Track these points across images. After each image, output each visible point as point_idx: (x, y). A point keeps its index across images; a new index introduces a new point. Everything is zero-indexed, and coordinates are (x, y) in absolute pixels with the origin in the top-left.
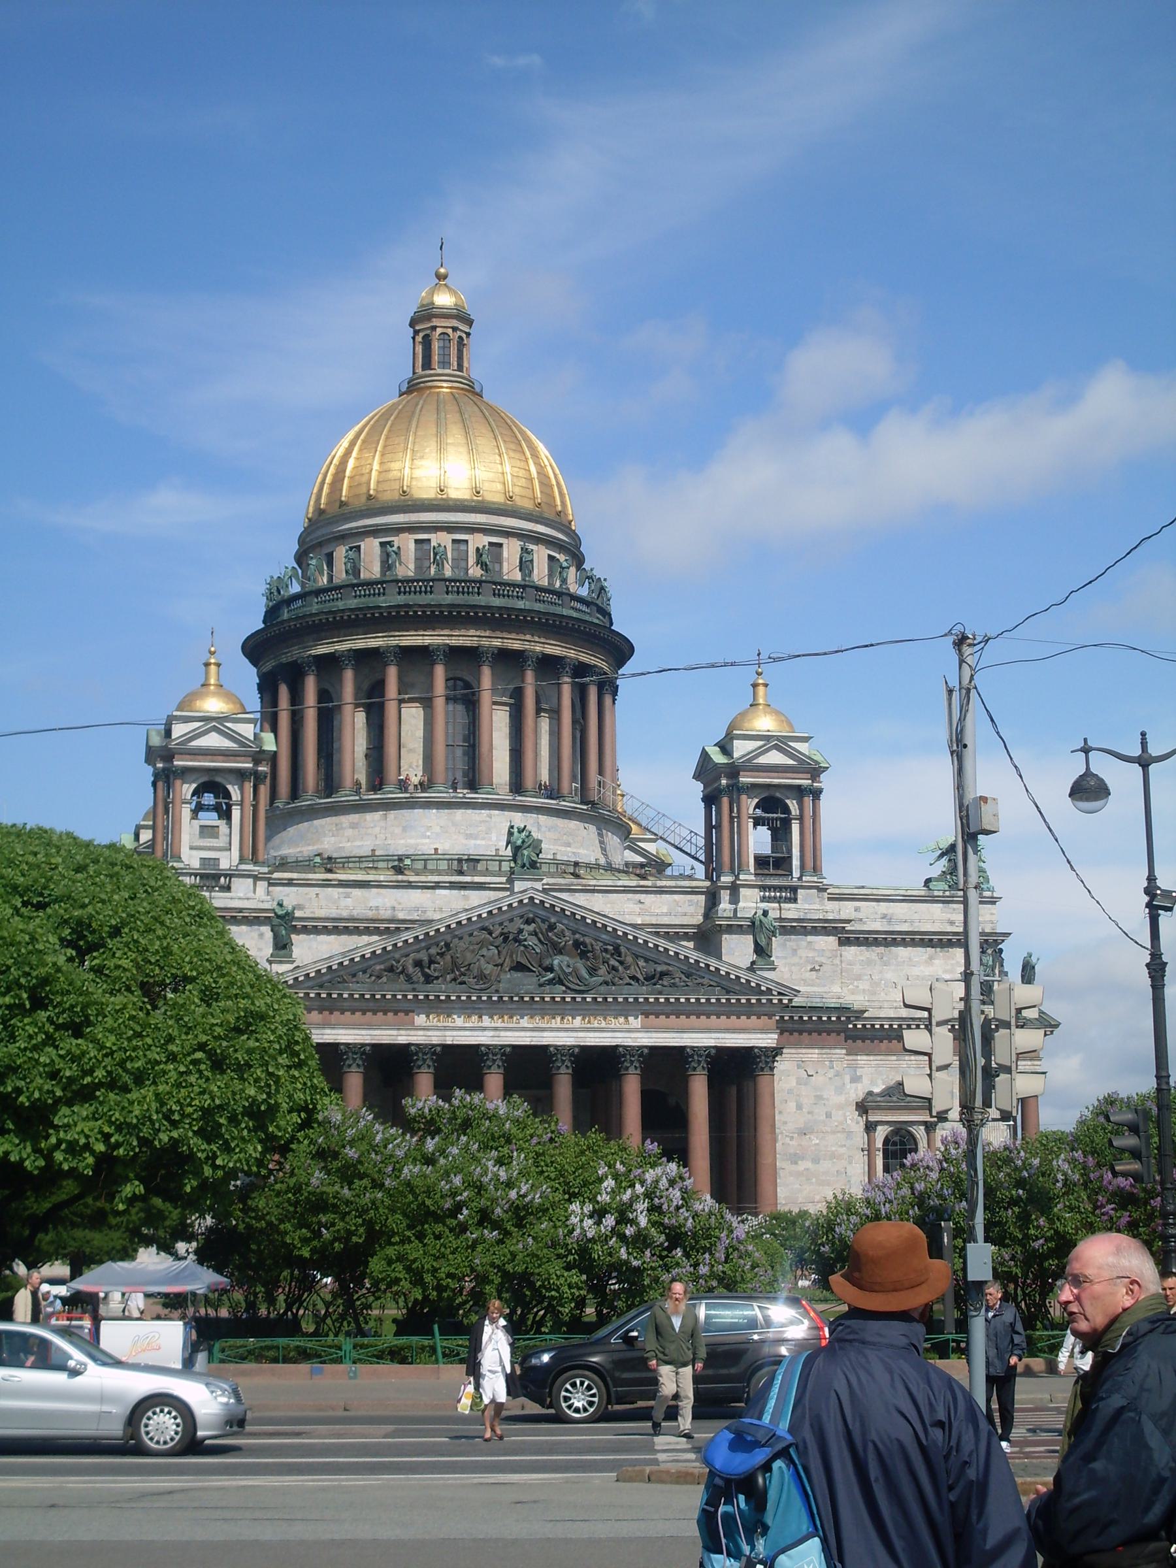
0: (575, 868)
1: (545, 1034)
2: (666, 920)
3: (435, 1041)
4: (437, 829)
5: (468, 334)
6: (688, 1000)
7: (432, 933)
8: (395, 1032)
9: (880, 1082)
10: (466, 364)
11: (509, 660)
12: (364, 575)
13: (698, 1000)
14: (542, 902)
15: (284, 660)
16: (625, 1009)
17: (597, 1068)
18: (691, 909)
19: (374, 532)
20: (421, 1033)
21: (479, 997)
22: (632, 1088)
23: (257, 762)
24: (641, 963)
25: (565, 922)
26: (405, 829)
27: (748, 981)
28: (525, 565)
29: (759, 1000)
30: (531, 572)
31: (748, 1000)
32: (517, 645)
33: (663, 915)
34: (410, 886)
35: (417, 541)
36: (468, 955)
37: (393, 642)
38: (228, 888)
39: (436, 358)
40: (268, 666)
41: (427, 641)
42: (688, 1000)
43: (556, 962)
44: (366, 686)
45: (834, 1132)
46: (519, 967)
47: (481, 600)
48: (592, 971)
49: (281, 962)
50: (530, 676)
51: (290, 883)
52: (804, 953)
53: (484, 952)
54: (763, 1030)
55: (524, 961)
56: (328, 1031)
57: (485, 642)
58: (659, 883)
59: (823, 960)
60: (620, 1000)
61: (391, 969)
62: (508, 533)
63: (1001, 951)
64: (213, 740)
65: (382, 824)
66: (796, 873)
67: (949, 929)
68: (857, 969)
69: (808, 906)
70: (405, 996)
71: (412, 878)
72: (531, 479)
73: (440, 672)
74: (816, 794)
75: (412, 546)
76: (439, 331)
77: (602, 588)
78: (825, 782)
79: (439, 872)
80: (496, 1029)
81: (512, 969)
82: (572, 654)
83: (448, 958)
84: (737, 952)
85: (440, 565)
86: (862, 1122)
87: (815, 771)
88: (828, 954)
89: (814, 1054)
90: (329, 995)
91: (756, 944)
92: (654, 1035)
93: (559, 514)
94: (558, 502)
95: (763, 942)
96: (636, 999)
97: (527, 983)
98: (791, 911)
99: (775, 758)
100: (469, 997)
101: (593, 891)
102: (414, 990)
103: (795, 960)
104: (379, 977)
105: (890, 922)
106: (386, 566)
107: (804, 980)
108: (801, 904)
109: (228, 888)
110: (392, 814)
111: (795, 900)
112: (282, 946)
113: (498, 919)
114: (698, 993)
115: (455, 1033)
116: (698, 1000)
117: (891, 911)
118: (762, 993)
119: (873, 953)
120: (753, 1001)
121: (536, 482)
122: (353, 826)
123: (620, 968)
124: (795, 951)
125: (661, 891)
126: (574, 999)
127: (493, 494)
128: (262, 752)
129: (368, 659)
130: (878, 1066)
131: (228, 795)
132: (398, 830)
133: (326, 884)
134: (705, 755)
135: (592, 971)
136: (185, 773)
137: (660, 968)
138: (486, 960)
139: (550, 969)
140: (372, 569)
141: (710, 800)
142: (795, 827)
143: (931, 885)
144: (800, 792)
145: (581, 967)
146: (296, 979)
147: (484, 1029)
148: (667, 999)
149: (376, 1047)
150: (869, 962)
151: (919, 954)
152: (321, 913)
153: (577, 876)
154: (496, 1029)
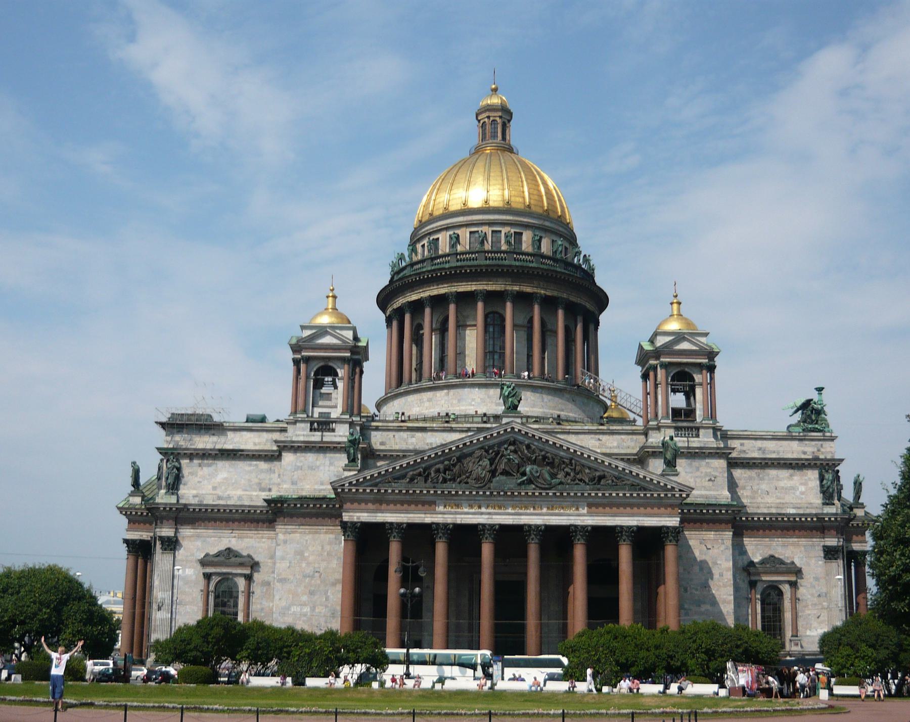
0: (559, 420)
1: (523, 517)
2: (616, 451)
3: (449, 521)
4: (479, 400)
5: (509, 121)
6: (618, 494)
7: (447, 451)
8: (423, 515)
9: (758, 555)
10: (508, 138)
11: (523, 300)
12: (440, 252)
13: (624, 494)
14: (520, 431)
15: (395, 306)
16: (576, 502)
17: (558, 540)
18: (632, 444)
19: (447, 228)
20: (440, 516)
21: (477, 493)
22: (579, 552)
23: (353, 353)
24: (587, 471)
25: (536, 443)
26: (459, 401)
27: (659, 483)
28: (538, 242)
29: (666, 495)
30: (539, 247)
31: (659, 495)
32: (528, 290)
33: (614, 447)
34: (451, 430)
35: (471, 233)
36: (471, 464)
37: (454, 289)
38: (333, 430)
39: (488, 135)
40: (388, 313)
41: (474, 288)
42: (618, 494)
43: (528, 469)
44: (440, 320)
45: (725, 586)
46: (505, 473)
47: (506, 262)
48: (553, 476)
49: (350, 470)
50: (536, 308)
51: (377, 429)
52: (702, 469)
53: (481, 463)
54: (670, 515)
55: (507, 469)
56: (380, 515)
57: (509, 288)
58: (611, 428)
59: (717, 474)
60: (572, 494)
61: (420, 474)
62: (527, 226)
63: (838, 471)
64: (327, 340)
65: (446, 398)
66: (698, 420)
67: (803, 456)
69: (706, 439)
70: (428, 492)
71: (454, 425)
72: (541, 196)
73: (480, 305)
74: (711, 369)
75: (468, 235)
76: (491, 119)
77: (586, 260)
78: (718, 360)
79: (472, 423)
80: (489, 514)
81: (502, 474)
82: (565, 296)
83: (457, 467)
84: (657, 466)
85: (482, 243)
86: (746, 582)
87: (711, 355)
88: (720, 470)
89: (711, 535)
90: (379, 491)
91: (665, 459)
92: (596, 518)
93: (560, 217)
94: (559, 210)
96: (582, 494)
97: (510, 483)
98: (695, 443)
99: (685, 346)
100: (471, 492)
101: (569, 433)
102: (434, 487)
103: (698, 474)
104: (412, 480)
105: (764, 453)
106: (453, 246)
107: (704, 487)
108: (701, 438)
109: (333, 430)
110: (452, 392)
111: (698, 436)
112: (352, 460)
113: (491, 442)
114: (624, 489)
115: (462, 516)
116: (624, 494)
117: (764, 446)
118: (669, 490)
119: (753, 473)
120: (662, 495)
121: (544, 198)
122: (430, 400)
123: (572, 474)
124: (698, 469)
125: (612, 433)
126: (540, 494)
127: (517, 203)
128: (356, 347)
129: (439, 302)
130: (757, 545)
131: (336, 374)
132: (455, 402)
133: (399, 429)
134: (641, 347)
135: (553, 476)
136: (307, 360)
137: (598, 474)
138: (480, 468)
139: (524, 474)
140: (444, 246)
141: (645, 377)
142: (699, 391)
143: (791, 429)
144: (700, 365)
145: (546, 471)
146: (357, 481)
147: (482, 514)
148: (603, 494)
149: (411, 526)
150: (751, 478)
151: (784, 473)
152: (397, 447)
153: (559, 424)
154: (489, 514)
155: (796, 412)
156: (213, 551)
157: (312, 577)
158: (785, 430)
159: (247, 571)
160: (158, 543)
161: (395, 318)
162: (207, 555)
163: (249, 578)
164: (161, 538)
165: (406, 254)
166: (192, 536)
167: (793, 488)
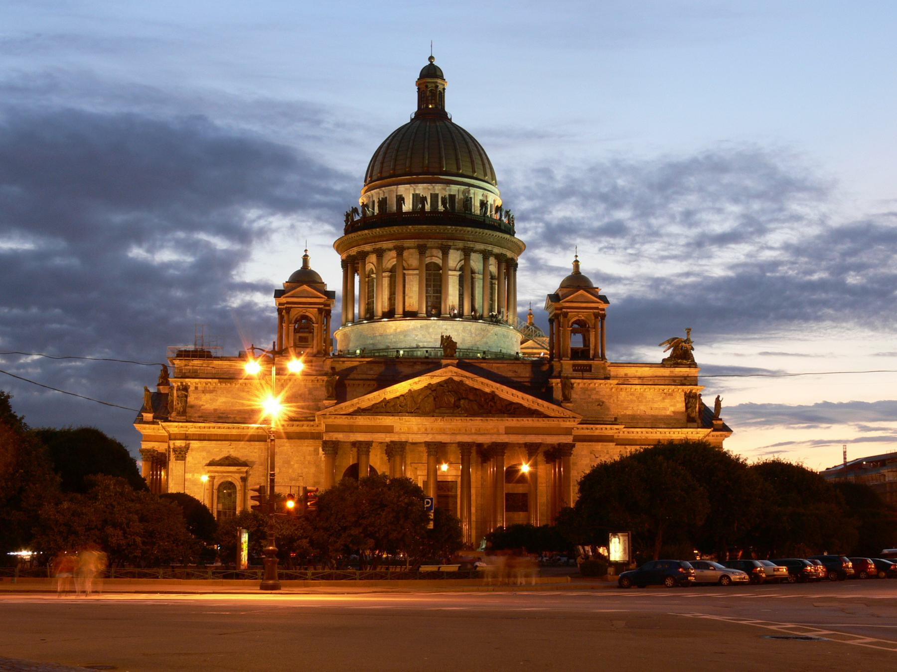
5: (444, 89)
68: (625, 404)
95: (567, 392)
115: (413, 436)
135: (481, 406)
155: (669, 349)
156: (217, 459)
157: (298, 480)
158: (660, 361)
159: (244, 475)
160: (172, 453)
161: (350, 266)
162: (211, 464)
163: (244, 480)
164: (175, 450)
165: (360, 211)
166: (199, 448)
167: (665, 409)
